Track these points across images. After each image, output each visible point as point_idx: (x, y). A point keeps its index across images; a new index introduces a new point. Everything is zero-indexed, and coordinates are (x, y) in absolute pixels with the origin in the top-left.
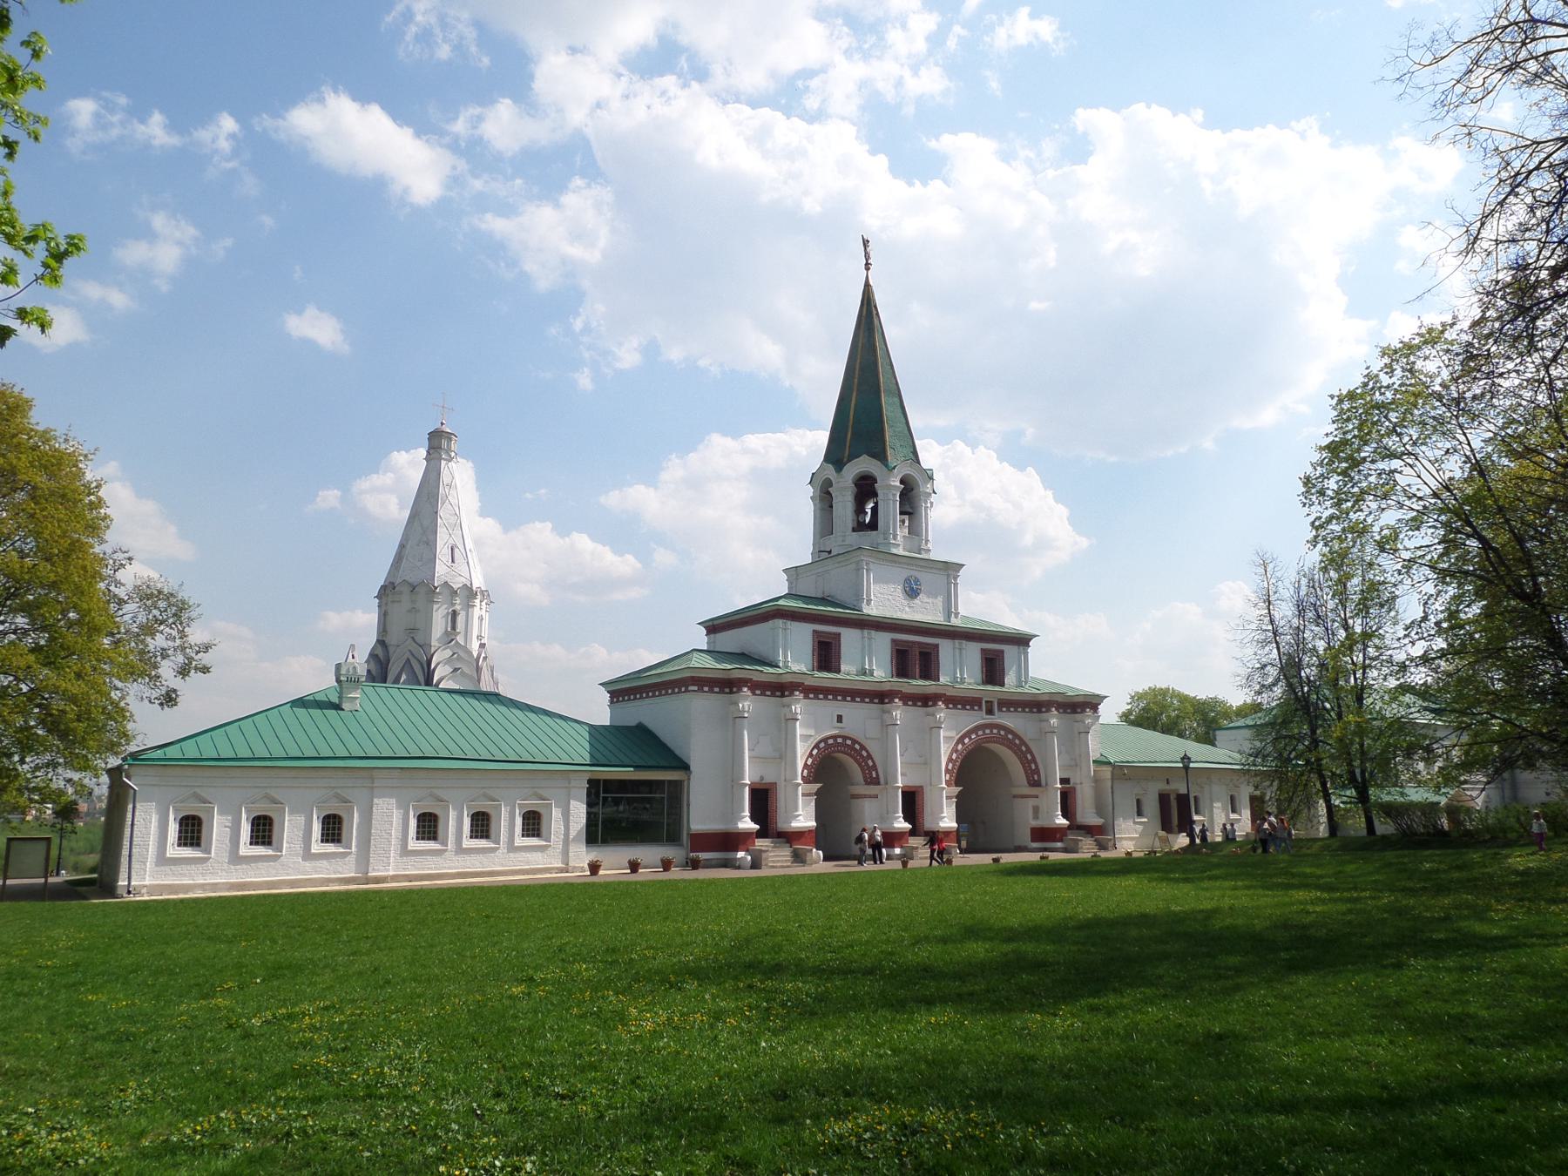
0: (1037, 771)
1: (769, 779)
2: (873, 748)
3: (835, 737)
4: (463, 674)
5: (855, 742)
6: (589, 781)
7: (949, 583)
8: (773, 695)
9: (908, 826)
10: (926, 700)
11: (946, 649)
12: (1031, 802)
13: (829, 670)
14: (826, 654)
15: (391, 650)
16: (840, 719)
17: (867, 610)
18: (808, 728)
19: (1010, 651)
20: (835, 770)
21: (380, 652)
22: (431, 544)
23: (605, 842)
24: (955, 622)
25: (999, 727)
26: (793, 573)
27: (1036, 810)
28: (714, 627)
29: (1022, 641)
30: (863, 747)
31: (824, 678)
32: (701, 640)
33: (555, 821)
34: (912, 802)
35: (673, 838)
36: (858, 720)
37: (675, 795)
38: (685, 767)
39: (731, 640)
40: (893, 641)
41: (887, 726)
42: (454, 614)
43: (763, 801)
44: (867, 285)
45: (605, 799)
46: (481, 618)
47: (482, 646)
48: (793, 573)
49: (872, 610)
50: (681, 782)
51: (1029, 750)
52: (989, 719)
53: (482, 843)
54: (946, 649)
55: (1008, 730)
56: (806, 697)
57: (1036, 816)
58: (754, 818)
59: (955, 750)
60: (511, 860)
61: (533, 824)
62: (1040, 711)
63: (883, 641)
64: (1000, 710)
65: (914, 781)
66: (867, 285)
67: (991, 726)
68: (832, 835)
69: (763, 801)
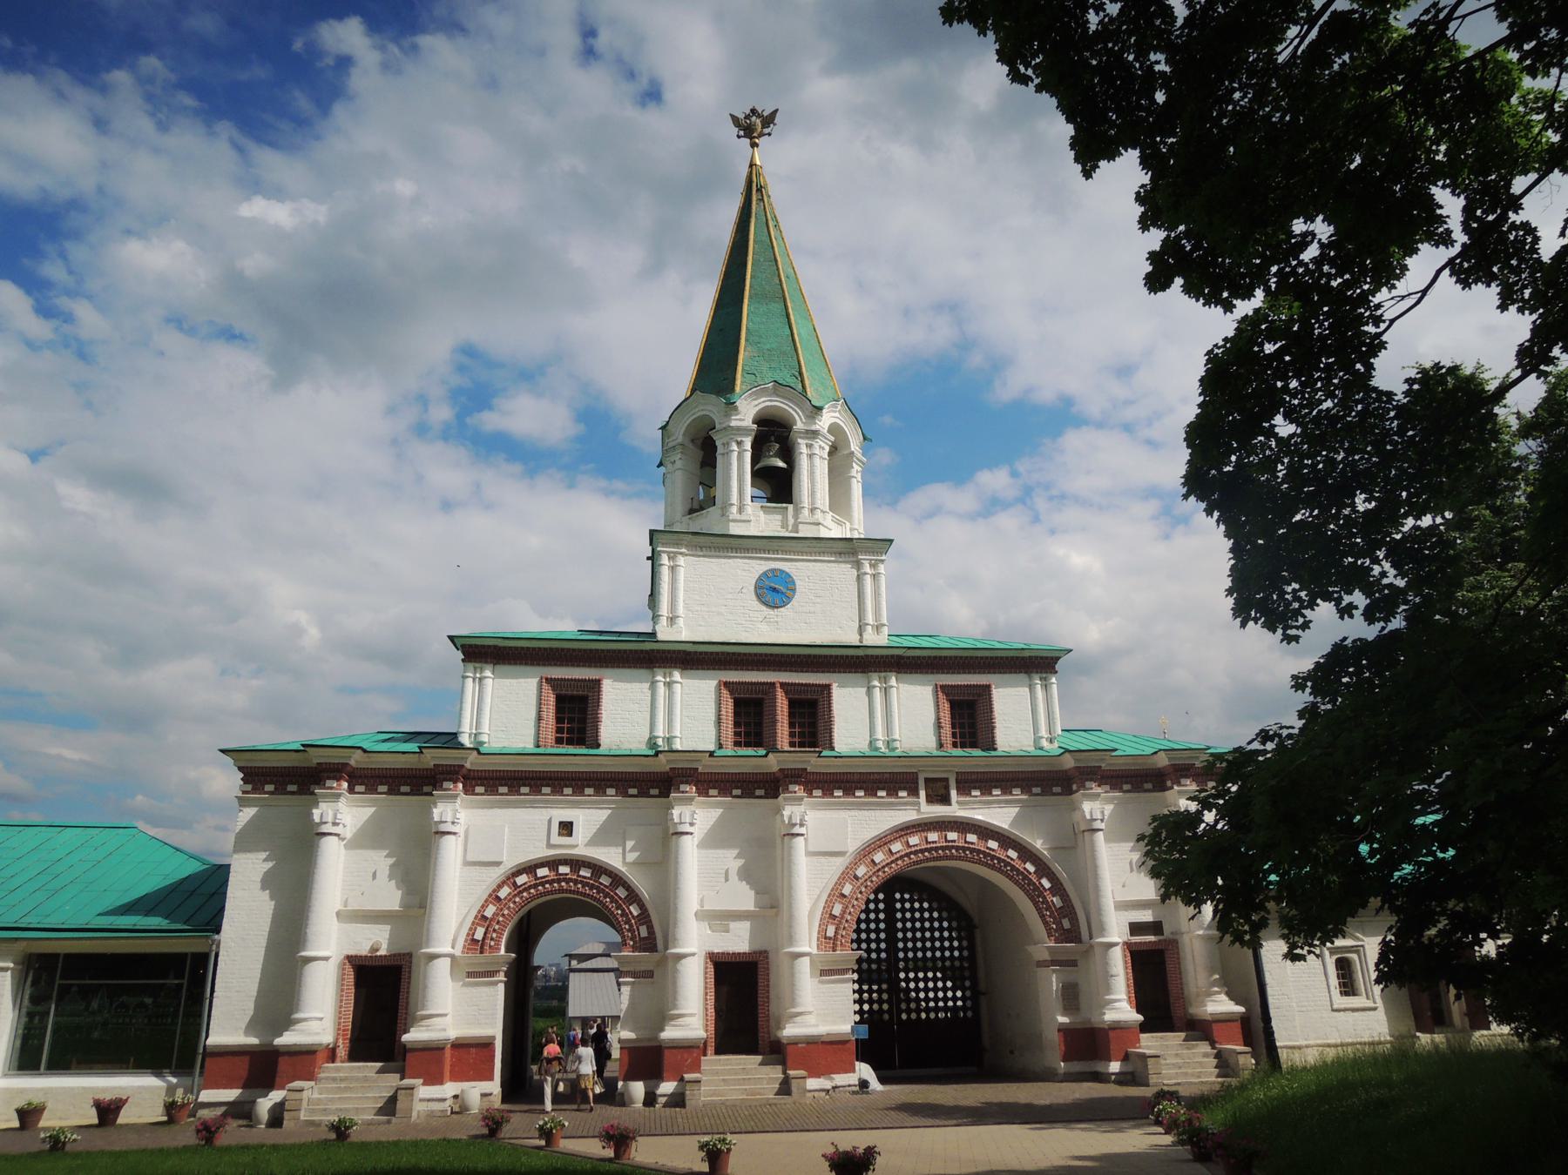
0: (1068, 910)
3: (553, 864)
7: (859, 579)
8: (416, 791)
10: (770, 786)
13: (581, 742)
14: (575, 714)
16: (567, 828)
18: (482, 843)
23: (59, 1065)
24: (871, 638)
25: (964, 826)
27: (1071, 997)
29: (1036, 664)
31: (574, 758)
43: (382, 991)
49: (680, 630)
52: (939, 811)
55: (986, 832)
56: (468, 790)
59: (849, 875)
65: (738, 941)
67: (941, 825)
69: (382, 991)
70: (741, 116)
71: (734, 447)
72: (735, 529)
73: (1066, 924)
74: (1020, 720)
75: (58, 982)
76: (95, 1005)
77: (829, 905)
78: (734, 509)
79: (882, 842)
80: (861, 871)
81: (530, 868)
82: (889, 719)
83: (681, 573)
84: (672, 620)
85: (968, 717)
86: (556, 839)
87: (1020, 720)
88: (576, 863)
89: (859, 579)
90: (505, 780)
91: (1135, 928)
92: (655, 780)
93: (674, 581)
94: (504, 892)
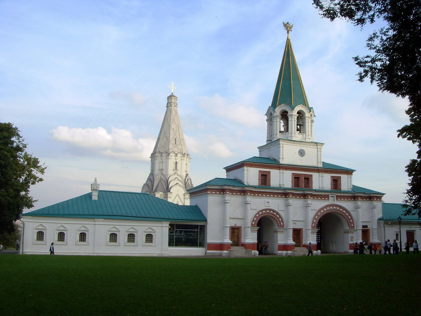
1: (237, 225)
2: (281, 213)
3: (266, 210)
4: (179, 185)
5: (274, 211)
6: (170, 225)
9: (294, 243)
10: (305, 196)
11: (315, 176)
12: (350, 235)
14: (265, 178)
15: (155, 176)
17: (281, 162)
19: (344, 177)
20: (265, 223)
21: (151, 178)
22: (168, 139)
23: (176, 245)
24: (320, 165)
27: (352, 238)
28: (228, 169)
30: (278, 214)
33: (156, 238)
34: (297, 233)
35: (201, 245)
36: (275, 204)
37: (203, 229)
38: (206, 220)
39: (234, 174)
40: (293, 174)
41: (288, 205)
42: (176, 163)
43: (235, 232)
44: (288, 39)
45: (176, 231)
46: (187, 164)
47: (187, 175)
50: (204, 225)
51: (350, 214)
53: (132, 244)
54: (315, 176)
57: (352, 240)
58: (232, 239)
59: (317, 214)
60: (140, 250)
61: (149, 238)
62: (355, 200)
64: (337, 199)
65: (298, 226)
68: (261, 246)
71: (293, 119)
72: (294, 139)
73: (352, 225)
74: (346, 184)
76: (182, 234)
77: (313, 220)
78: (293, 134)
79: (322, 209)
80: (319, 214)
81: (262, 211)
82: (322, 182)
83: (284, 148)
85: (336, 182)
87: (346, 184)
88: (270, 210)
90: (255, 192)
91: (364, 226)
92: (284, 194)
93: (283, 150)
94: (257, 215)
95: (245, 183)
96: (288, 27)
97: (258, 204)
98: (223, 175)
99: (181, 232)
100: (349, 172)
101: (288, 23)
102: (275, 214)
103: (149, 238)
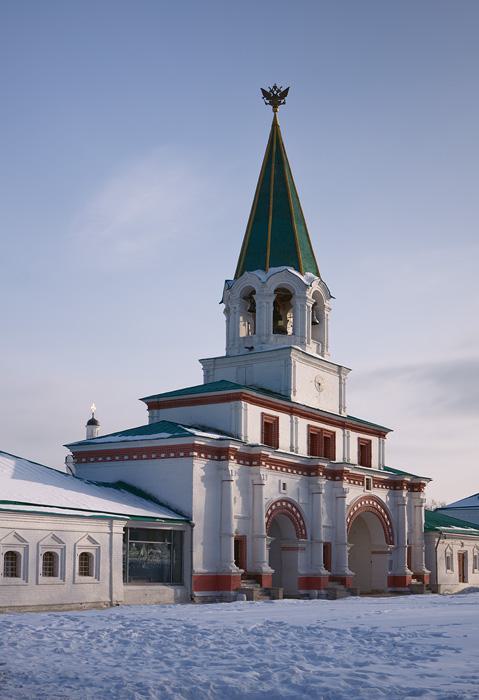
3: (281, 501)
6: (125, 529)
14: (270, 431)
26: (209, 364)
28: (154, 403)
32: (142, 417)
39: (168, 414)
44: (275, 125)
48: (209, 364)
63: (303, 424)
66: (275, 125)
70: (268, 90)
75: (129, 541)
76: (142, 553)
82: (346, 446)
84: (295, 392)
86: (282, 491)
89: (340, 383)
95: (243, 438)
96: (275, 98)
97: (274, 485)
98: (142, 417)
99: (139, 547)
100: (381, 432)
101: (275, 87)
102: (294, 509)
103: (86, 564)
